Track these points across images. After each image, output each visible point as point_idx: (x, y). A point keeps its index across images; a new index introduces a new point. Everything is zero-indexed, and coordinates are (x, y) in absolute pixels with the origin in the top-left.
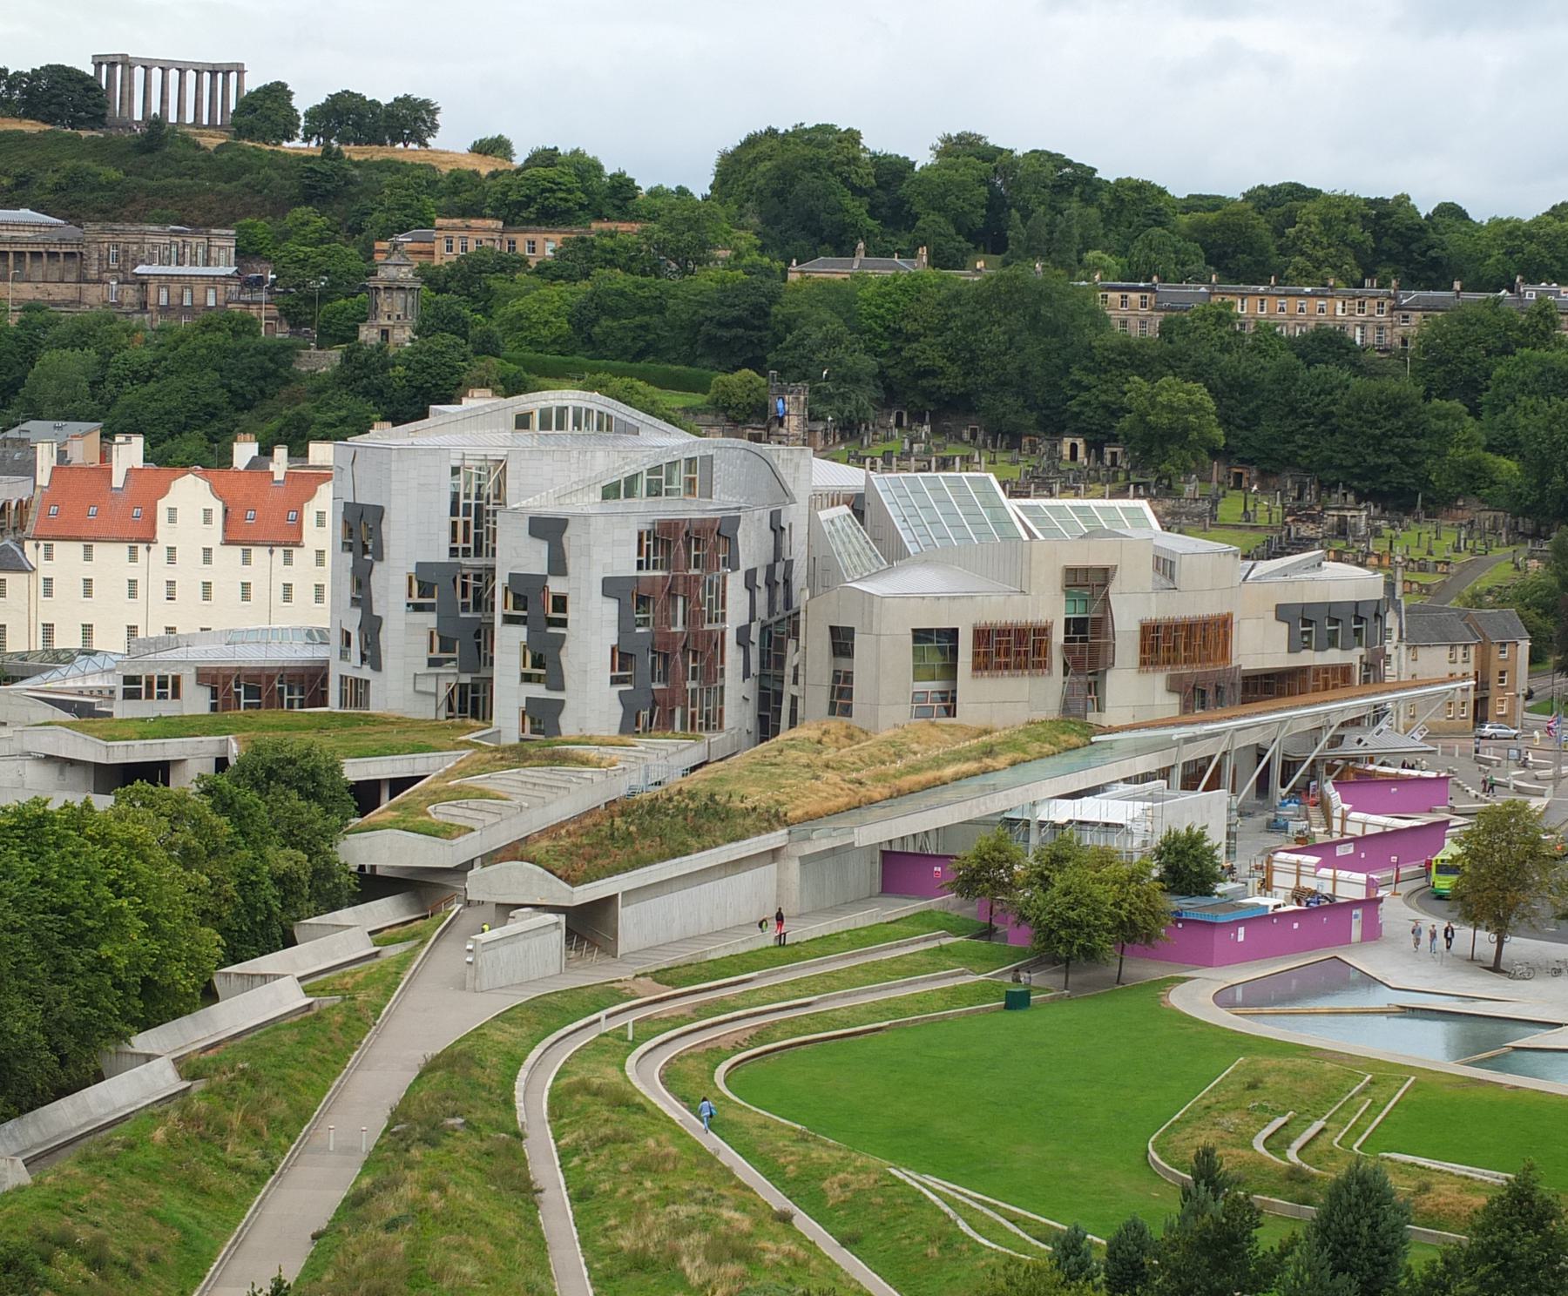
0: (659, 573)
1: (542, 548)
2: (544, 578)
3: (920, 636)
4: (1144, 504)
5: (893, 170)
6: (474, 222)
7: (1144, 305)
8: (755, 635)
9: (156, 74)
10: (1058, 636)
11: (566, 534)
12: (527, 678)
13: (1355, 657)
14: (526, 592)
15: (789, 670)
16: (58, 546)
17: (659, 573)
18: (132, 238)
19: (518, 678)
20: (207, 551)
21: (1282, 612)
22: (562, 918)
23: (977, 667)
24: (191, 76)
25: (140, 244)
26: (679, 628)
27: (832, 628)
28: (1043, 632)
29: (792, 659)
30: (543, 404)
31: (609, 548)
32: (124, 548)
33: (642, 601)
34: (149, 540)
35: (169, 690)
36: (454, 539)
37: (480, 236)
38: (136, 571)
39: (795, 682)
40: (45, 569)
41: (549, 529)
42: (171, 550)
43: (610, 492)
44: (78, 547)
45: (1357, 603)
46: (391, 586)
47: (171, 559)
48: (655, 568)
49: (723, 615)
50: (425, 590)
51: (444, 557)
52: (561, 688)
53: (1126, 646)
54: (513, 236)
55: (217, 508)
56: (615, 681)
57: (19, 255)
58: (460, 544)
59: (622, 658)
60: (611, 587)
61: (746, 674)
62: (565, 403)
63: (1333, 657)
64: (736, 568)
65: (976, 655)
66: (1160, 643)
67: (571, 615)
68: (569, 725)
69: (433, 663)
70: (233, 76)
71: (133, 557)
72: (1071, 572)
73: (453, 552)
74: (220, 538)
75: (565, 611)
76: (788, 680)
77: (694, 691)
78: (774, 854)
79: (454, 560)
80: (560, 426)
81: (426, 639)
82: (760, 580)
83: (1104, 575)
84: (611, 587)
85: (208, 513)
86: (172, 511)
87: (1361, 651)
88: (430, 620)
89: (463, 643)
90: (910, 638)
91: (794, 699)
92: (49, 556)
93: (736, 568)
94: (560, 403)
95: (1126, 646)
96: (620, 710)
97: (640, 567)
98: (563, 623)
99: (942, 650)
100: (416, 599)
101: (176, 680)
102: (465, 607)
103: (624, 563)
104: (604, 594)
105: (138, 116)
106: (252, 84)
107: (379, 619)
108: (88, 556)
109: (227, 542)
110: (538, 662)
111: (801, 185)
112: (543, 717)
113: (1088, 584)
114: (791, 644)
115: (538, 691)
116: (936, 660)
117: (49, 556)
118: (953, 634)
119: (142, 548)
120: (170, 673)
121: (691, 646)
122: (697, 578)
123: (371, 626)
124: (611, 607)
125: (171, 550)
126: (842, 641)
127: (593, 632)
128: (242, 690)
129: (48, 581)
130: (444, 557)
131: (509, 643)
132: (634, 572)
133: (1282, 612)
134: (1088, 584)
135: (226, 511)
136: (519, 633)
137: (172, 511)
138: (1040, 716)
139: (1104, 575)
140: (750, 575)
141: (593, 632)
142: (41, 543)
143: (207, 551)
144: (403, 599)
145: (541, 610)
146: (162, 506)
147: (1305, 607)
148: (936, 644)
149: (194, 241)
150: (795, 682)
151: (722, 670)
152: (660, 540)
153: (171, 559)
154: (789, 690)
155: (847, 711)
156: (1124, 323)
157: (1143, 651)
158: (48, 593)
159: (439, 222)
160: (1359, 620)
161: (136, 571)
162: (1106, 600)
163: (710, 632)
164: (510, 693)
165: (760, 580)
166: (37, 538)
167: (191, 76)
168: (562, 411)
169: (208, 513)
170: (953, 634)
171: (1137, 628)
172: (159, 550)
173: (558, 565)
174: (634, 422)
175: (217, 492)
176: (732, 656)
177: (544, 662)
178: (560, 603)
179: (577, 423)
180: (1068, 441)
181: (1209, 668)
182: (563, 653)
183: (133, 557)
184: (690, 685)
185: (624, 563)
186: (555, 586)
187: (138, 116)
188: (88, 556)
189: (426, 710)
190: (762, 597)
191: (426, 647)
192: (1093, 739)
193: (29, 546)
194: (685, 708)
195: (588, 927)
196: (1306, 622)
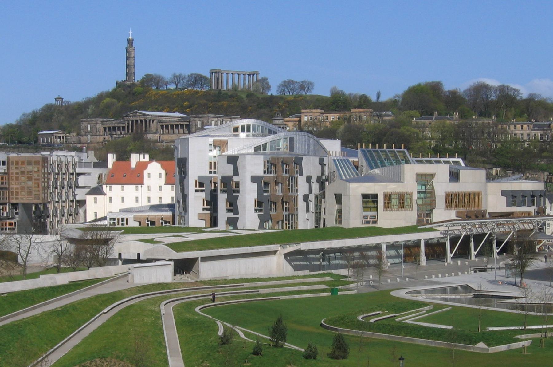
0: (272, 175)
1: (231, 166)
2: (232, 177)
3: (365, 196)
4: (460, 160)
5: (454, 93)
6: (314, 111)
7: (528, 129)
8: (312, 198)
9: (230, 76)
10: (415, 196)
12: (229, 210)
13: (532, 209)
14: (226, 180)
15: (323, 210)
16: (113, 186)
17: (272, 175)
18: (205, 119)
20: (160, 187)
21: (504, 193)
22: (172, 263)
23: (385, 207)
24: (242, 76)
25: (207, 120)
26: (280, 194)
27: (335, 195)
28: (411, 194)
29: (323, 205)
30: (242, 124)
31: (254, 166)
32: (134, 187)
33: (266, 184)
34: (141, 183)
35: (125, 223)
36: (211, 168)
37: (316, 115)
38: (138, 194)
39: (325, 213)
40: (109, 194)
41: (233, 160)
42: (149, 187)
43: (257, 149)
44: (120, 187)
45: (532, 191)
47: (149, 190)
48: (271, 173)
49: (297, 190)
50: (201, 185)
51: (207, 174)
52: (238, 213)
53: (440, 201)
54: (327, 115)
55: (163, 172)
56: (256, 210)
57: (172, 126)
58: (213, 170)
59: (259, 204)
60: (254, 179)
61: (308, 210)
62: (249, 124)
63: (524, 209)
64: (301, 174)
65: (385, 203)
66: (452, 200)
67: (241, 188)
68: (239, 225)
69: (204, 209)
70: (255, 75)
71: (137, 190)
72: (418, 175)
73: (210, 172)
74: (164, 183)
75: (238, 187)
76: (322, 213)
77: (286, 215)
78: (275, 252)
79: (211, 175)
80: (248, 131)
82: (314, 179)
83: (432, 175)
84: (254, 179)
85: (160, 174)
87: (535, 207)
88: (203, 195)
89: (212, 203)
90: (360, 197)
91: (324, 219)
92: (110, 190)
93: (301, 174)
94: (248, 124)
95: (440, 201)
96: (259, 221)
97: (265, 172)
98: (238, 192)
99: (373, 201)
100: (198, 188)
101: (127, 219)
103: (259, 171)
104: (252, 182)
105: (225, 88)
106: (260, 77)
108: (123, 190)
109: (167, 183)
110: (231, 205)
111: (425, 99)
112: (233, 222)
113: (425, 180)
114: (323, 201)
115: (231, 215)
116: (371, 205)
117: (110, 190)
118: (376, 196)
119: (139, 186)
120: (125, 217)
121: (285, 200)
122: (286, 177)
123: (185, 198)
124: (255, 186)
125: (149, 187)
126: (338, 198)
127: (249, 195)
128: (149, 222)
129: (110, 198)
131: (222, 199)
132: (262, 174)
133: (504, 193)
134: (425, 180)
135: (166, 174)
136: (225, 196)
137: (149, 175)
138: (409, 224)
139: (432, 175)
140: (309, 179)
141: (249, 195)
142: (108, 186)
143: (160, 187)
145: (231, 187)
146: (146, 172)
147: (512, 191)
148: (370, 200)
149: (226, 119)
150: (325, 213)
151: (297, 209)
152: (272, 164)
153: (149, 190)
154: (323, 216)
155: (340, 222)
156: (522, 135)
157: (446, 202)
158: (111, 202)
159: (303, 111)
160: (533, 196)
161: (138, 194)
162: (433, 185)
163: (292, 196)
164: (223, 215)
165: (314, 179)
166: (107, 184)
167: (242, 76)
168: (248, 126)
169: (160, 175)
170: (376, 196)
171: (444, 194)
172: (145, 187)
173: (236, 172)
174: (275, 130)
175: (163, 167)
176: (301, 205)
177: (233, 206)
178: (237, 184)
179: (254, 130)
180: (494, 169)
181: (472, 209)
183: (137, 190)
184: (285, 213)
185: (259, 171)
186: (235, 179)
187: (225, 88)
188: (123, 190)
189: (202, 224)
190: (315, 187)
192: (205, 128)
193: (104, 186)
194: (283, 221)
195: (183, 267)
196: (513, 197)
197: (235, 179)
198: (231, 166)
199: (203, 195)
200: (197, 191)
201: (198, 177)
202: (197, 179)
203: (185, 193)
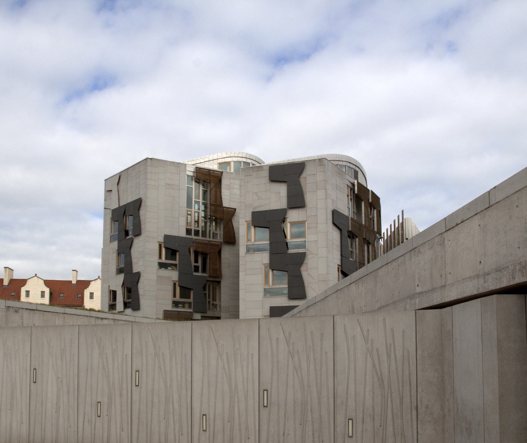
1: (282, 189)
11: (304, 175)
19: (262, 294)
46: (146, 254)
50: (172, 253)
51: (183, 233)
55: (47, 291)
60: (337, 219)
67: (310, 237)
69: (176, 304)
73: (188, 231)
81: (170, 288)
86: (28, 293)
102: (196, 269)
107: (138, 274)
124: (335, 235)
130: (183, 233)
137: (28, 293)
144: (156, 260)
169: (43, 294)
173: (297, 200)
182: (303, 269)
191: (171, 294)
197: (293, 216)
198: (282, 189)
199: (173, 275)
200: (162, 265)
201: (166, 237)
202: (161, 239)
203: (135, 270)
